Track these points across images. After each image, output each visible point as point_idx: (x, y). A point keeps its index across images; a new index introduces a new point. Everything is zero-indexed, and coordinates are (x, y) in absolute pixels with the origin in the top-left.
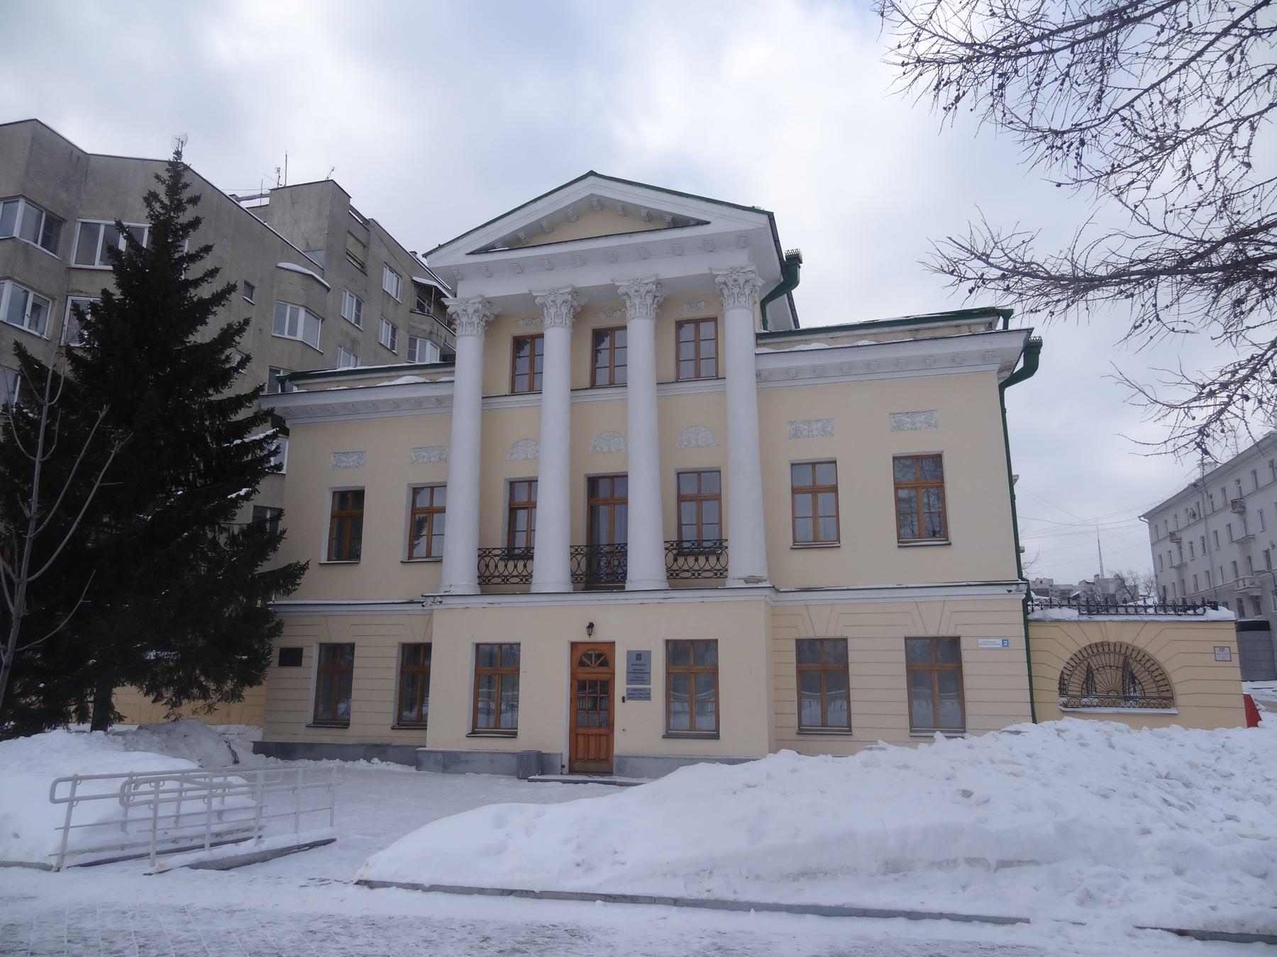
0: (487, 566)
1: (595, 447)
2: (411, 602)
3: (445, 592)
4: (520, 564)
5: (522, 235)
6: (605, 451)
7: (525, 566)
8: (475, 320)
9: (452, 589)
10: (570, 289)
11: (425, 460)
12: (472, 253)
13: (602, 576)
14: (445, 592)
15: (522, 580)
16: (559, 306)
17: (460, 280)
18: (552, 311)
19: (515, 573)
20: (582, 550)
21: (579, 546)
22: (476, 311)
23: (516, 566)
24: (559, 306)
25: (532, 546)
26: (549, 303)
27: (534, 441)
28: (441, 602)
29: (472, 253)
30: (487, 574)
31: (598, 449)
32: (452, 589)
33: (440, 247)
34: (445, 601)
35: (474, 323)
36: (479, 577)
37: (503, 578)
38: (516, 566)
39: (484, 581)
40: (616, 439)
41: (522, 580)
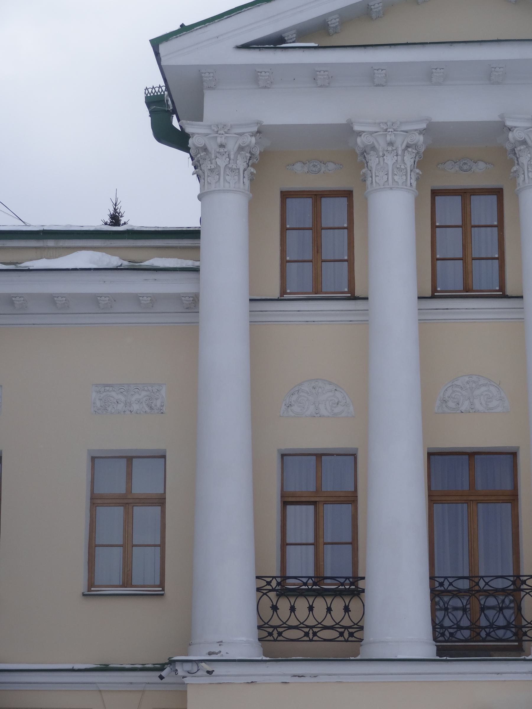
0: (275, 608)
1: (445, 401)
2: (105, 669)
3: (210, 654)
4: (338, 604)
5: (334, 22)
6: (463, 408)
7: (347, 609)
8: (241, 164)
9: (222, 649)
10: (423, 126)
11: (120, 407)
12: (246, 46)
13: (524, 630)
14: (210, 654)
15: (342, 634)
16: (400, 152)
17: (210, 88)
18: (390, 160)
19: (329, 622)
20: (451, 584)
21: (446, 578)
22: (241, 149)
23: (329, 610)
24: (400, 152)
25: (360, 575)
26: (381, 144)
27: (330, 383)
28: (209, 673)
29: (246, 46)
30: (275, 622)
31: (451, 404)
32: (222, 649)
33: (184, 29)
34: (219, 669)
35: (239, 169)
36: (259, 627)
37: (307, 630)
38: (329, 610)
39: (270, 634)
40: (483, 389)
41: (342, 634)
